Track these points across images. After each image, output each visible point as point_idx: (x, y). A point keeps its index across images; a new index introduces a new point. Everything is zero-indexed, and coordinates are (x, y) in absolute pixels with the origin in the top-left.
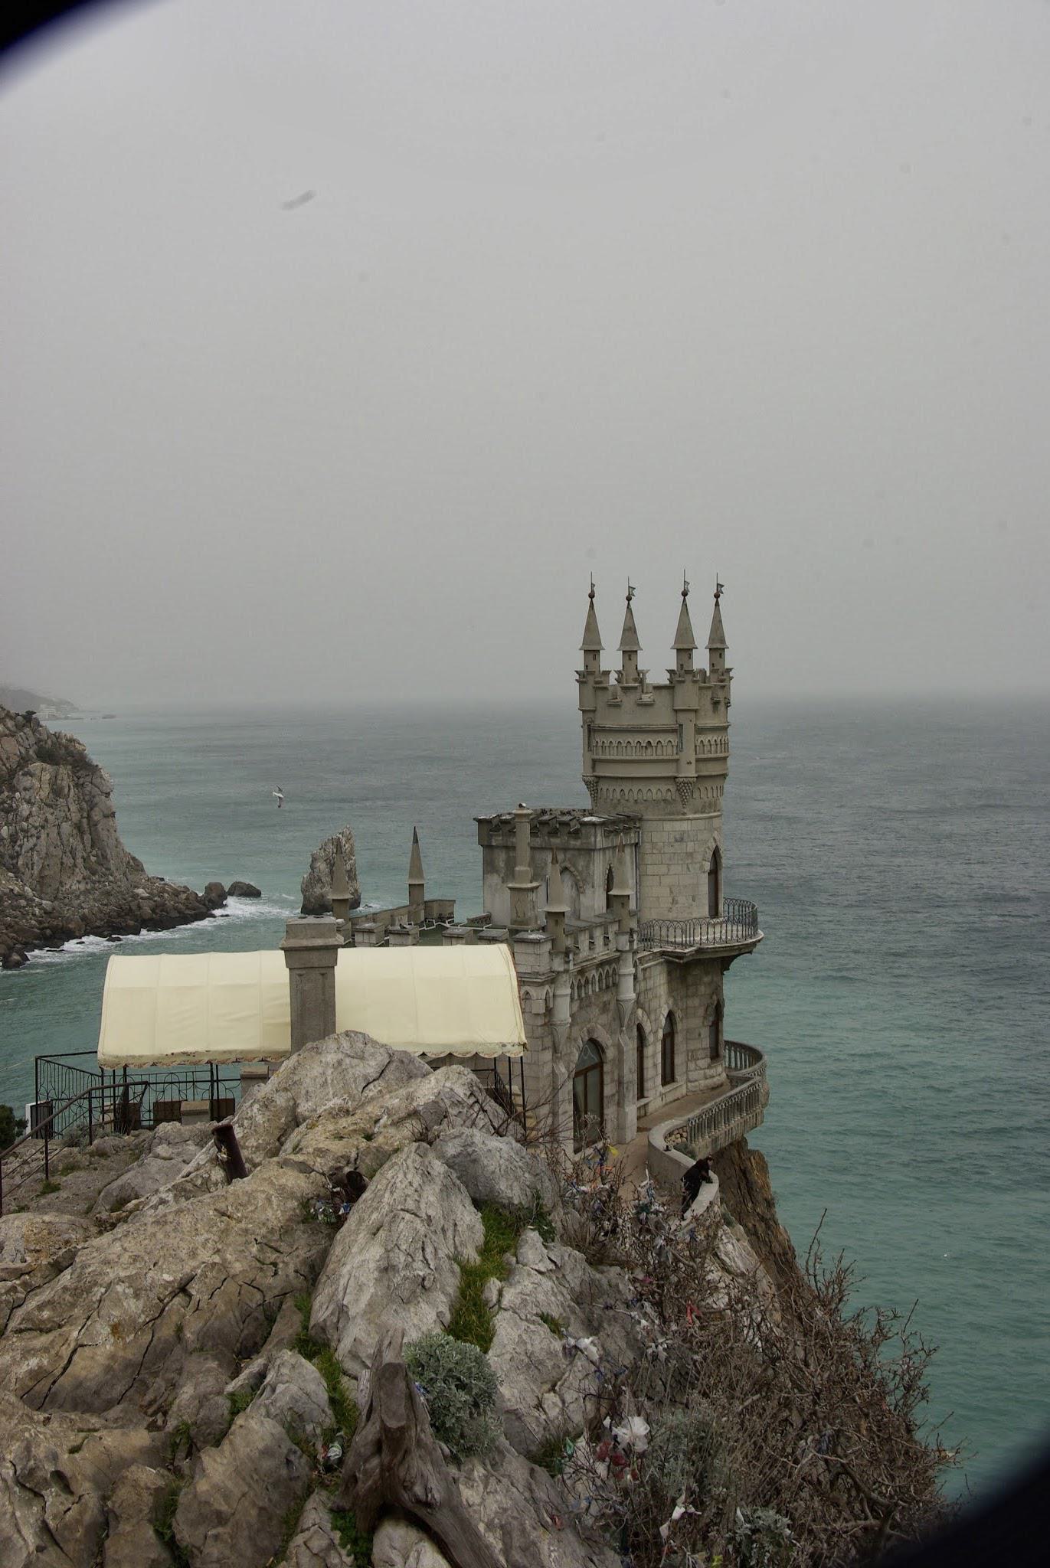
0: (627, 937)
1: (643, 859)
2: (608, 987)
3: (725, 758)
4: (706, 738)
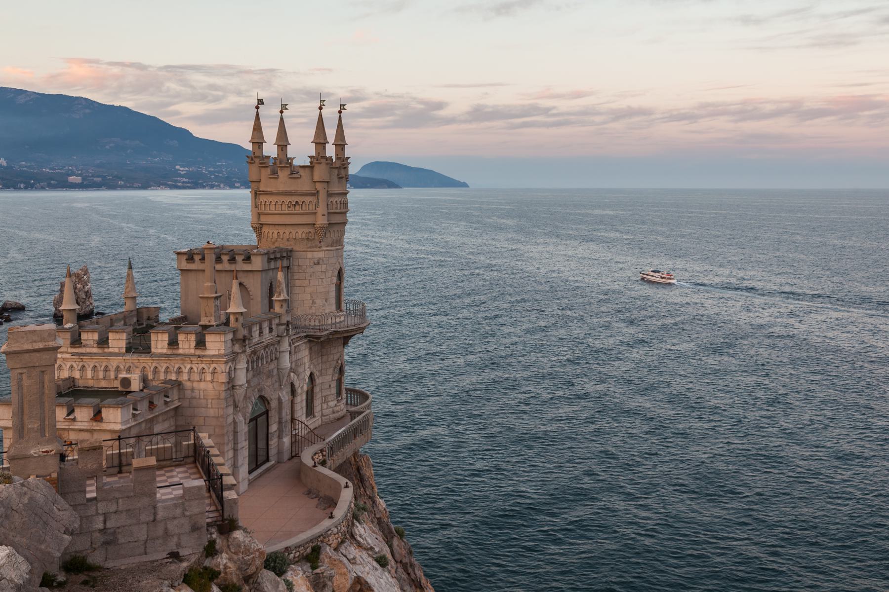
0: (284, 327)
1: (292, 276)
2: (272, 360)
3: (345, 213)
4: (334, 200)
